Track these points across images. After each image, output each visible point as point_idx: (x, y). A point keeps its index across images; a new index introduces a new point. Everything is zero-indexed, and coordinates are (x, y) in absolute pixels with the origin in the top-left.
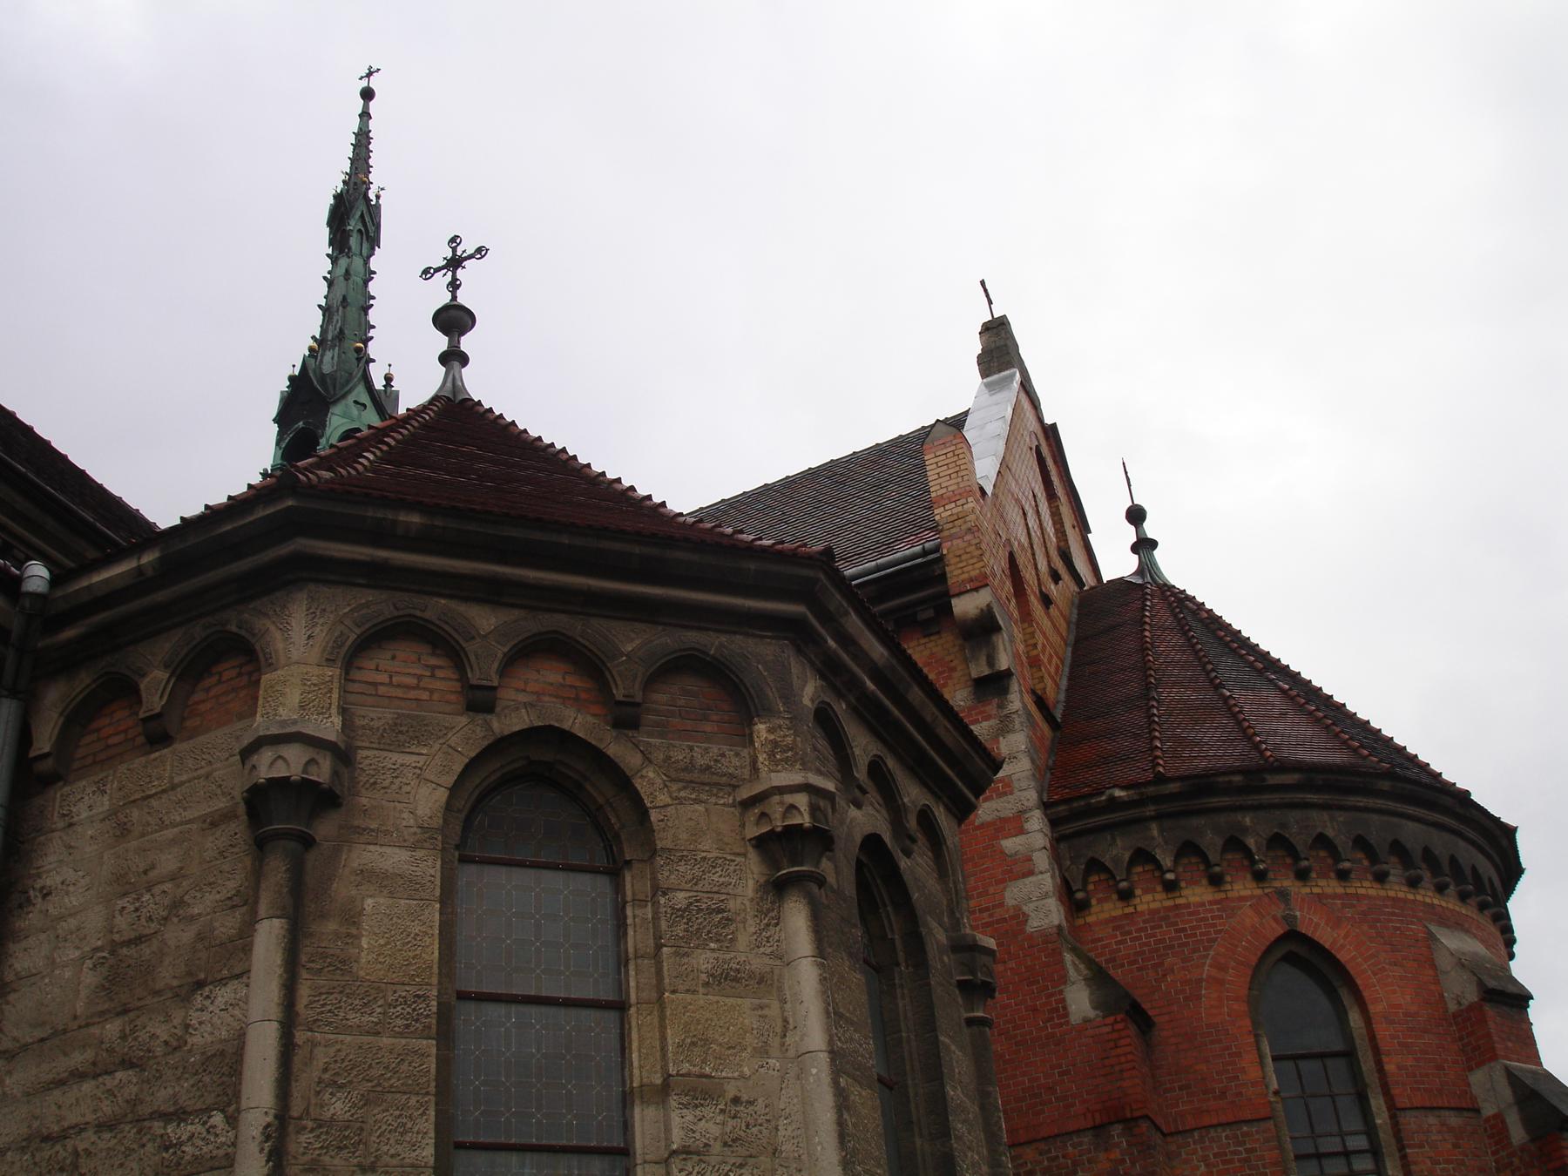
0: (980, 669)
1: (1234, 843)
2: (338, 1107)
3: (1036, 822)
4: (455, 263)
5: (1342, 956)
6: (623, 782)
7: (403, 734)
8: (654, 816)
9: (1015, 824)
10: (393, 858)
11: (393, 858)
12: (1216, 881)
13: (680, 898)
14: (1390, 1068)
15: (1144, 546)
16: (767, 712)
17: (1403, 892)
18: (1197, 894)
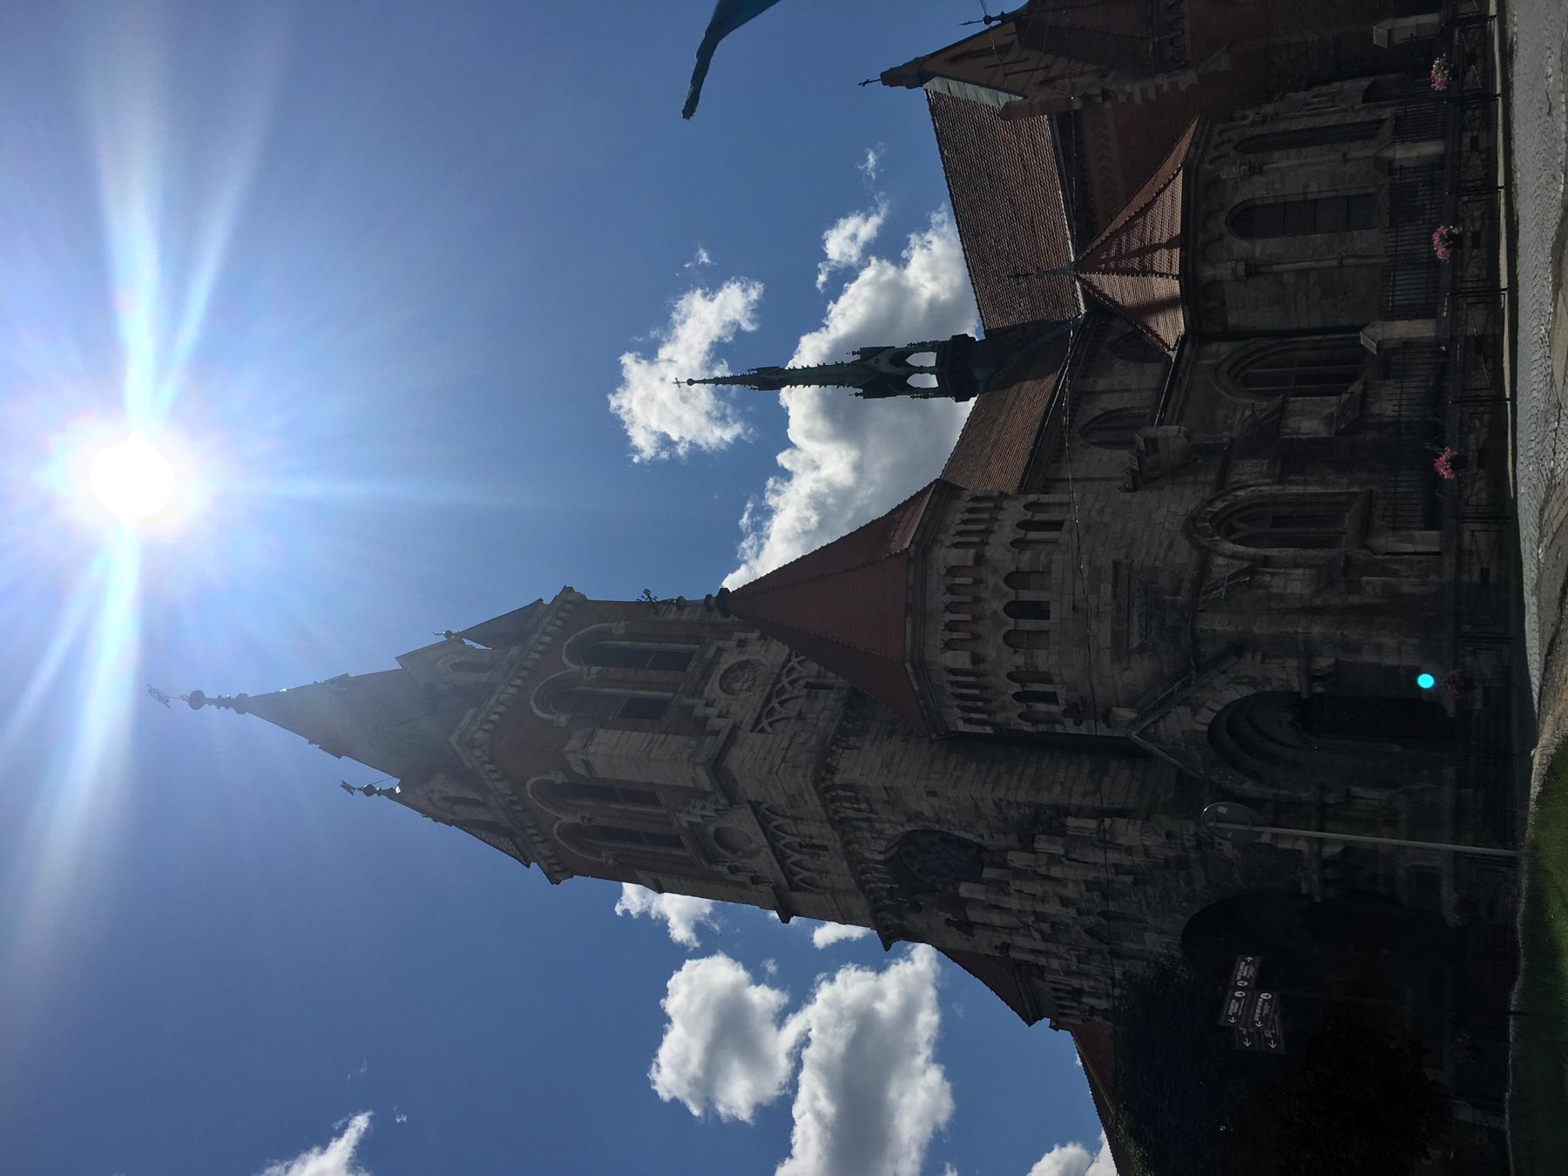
0: (1100, 99)
4: (1017, 276)
6: (1236, 206)
8: (1245, 199)
10: (1258, 250)
11: (1258, 250)
13: (1264, 192)
16: (1219, 176)
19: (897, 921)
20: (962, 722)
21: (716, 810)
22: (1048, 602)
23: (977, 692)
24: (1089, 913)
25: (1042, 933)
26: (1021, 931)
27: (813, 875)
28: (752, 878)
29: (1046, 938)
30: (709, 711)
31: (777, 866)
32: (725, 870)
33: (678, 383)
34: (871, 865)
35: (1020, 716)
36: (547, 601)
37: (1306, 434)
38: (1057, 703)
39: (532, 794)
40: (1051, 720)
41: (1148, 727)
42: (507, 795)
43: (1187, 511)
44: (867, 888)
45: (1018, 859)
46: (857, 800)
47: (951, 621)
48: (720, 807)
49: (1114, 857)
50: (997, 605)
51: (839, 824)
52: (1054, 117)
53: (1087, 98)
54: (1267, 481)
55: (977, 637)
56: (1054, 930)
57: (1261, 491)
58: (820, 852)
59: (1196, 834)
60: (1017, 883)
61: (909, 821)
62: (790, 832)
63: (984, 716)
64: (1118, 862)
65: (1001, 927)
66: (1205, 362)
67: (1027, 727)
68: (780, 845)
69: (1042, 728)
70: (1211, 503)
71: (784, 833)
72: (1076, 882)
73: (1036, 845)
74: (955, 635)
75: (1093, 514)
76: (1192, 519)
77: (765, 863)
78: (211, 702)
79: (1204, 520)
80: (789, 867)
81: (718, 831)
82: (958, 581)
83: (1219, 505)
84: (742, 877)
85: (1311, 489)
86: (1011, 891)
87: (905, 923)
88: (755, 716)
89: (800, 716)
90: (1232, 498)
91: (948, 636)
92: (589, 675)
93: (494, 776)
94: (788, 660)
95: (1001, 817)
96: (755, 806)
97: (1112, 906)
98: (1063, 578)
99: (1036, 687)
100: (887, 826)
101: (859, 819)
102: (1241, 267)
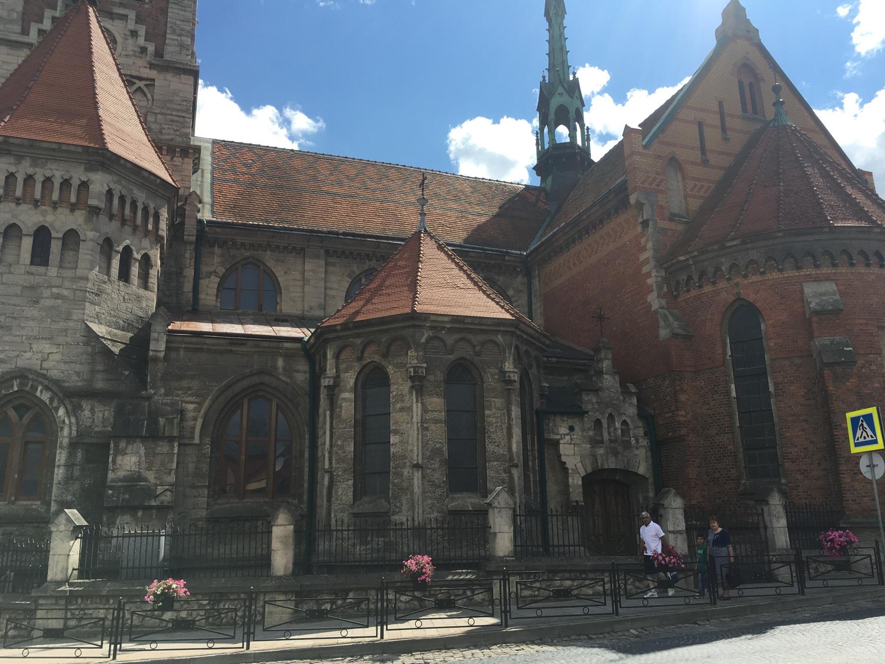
0: (640, 220)
2: (339, 443)
9: (649, 275)
12: (714, 283)
13: (394, 393)
16: (410, 348)
37: (114, 462)
43: (47, 370)
53: (640, 206)
54: (74, 433)
57: (62, 429)
66: (280, 363)
75: (55, 290)
76: (22, 375)
79: (21, 385)
83: (45, 397)
85: (59, 473)
90: (54, 405)
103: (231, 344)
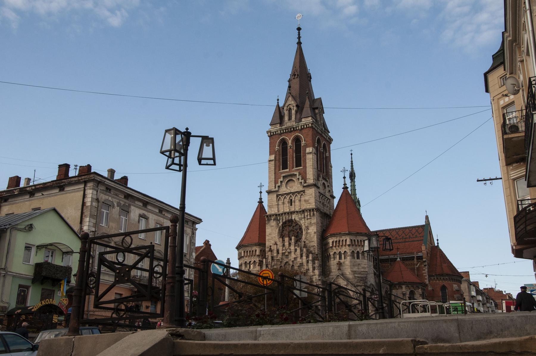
0: (425, 264)
1: (441, 278)
3: (427, 276)
4: (398, 249)
5: (447, 287)
7: (407, 291)
9: (426, 276)
12: (439, 281)
14: (449, 294)
15: (438, 243)
17: (452, 282)
18: (438, 281)
19: (272, 219)
20: (333, 241)
21: (301, 182)
22: (359, 259)
23: (341, 244)
24: (293, 263)
25: (285, 253)
26: (284, 248)
27: (283, 201)
28: (280, 186)
29: (283, 254)
30: (321, 181)
31: (284, 193)
32: (282, 180)
33: (351, 151)
34: (290, 216)
35: (335, 253)
36: (329, 134)
38: (339, 259)
39: (297, 135)
40: (334, 258)
41: (340, 277)
42: (296, 128)
44: (284, 214)
45: (305, 250)
46: (311, 216)
47: (355, 241)
48: (303, 184)
49: (311, 269)
50: (358, 250)
51: (303, 211)
52: (422, 255)
53: (425, 261)
55: (353, 245)
56: (286, 255)
58: (290, 204)
59: (320, 284)
60: (299, 249)
61: (306, 227)
62: (296, 198)
63: (335, 245)
64: (310, 270)
65: (284, 244)
67: (332, 253)
68: (291, 194)
69: (332, 256)
70: (374, 288)
71: (295, 197)
72: (302, 261)
73: (311, 254)
74: (353, 241)
76: (373, 285)
77: (284, 190)
78: (299, 34)
80: (284, 196)
81: (293, 180)
82: (362, 242)
83: (374, 289)
84: (279, 184)
86: (296, 248)
87: (272, 221)
88: (320, 192)
89: (320, 202)
91: (353, 240)
92: (322, 150)
93: (302, 127)
94: (327, 197)
95: (311, 246)
96: (304, 191)
97: (296, 268)
98: (364, 262)
99: (343, 256)
100: (304, 221)
101: (304, 216)
102: (405, 293)
103: (386, 282)
